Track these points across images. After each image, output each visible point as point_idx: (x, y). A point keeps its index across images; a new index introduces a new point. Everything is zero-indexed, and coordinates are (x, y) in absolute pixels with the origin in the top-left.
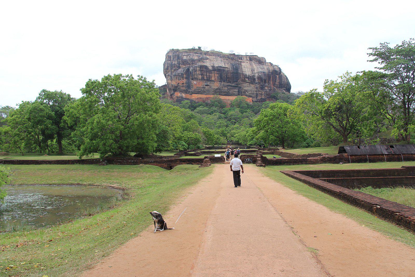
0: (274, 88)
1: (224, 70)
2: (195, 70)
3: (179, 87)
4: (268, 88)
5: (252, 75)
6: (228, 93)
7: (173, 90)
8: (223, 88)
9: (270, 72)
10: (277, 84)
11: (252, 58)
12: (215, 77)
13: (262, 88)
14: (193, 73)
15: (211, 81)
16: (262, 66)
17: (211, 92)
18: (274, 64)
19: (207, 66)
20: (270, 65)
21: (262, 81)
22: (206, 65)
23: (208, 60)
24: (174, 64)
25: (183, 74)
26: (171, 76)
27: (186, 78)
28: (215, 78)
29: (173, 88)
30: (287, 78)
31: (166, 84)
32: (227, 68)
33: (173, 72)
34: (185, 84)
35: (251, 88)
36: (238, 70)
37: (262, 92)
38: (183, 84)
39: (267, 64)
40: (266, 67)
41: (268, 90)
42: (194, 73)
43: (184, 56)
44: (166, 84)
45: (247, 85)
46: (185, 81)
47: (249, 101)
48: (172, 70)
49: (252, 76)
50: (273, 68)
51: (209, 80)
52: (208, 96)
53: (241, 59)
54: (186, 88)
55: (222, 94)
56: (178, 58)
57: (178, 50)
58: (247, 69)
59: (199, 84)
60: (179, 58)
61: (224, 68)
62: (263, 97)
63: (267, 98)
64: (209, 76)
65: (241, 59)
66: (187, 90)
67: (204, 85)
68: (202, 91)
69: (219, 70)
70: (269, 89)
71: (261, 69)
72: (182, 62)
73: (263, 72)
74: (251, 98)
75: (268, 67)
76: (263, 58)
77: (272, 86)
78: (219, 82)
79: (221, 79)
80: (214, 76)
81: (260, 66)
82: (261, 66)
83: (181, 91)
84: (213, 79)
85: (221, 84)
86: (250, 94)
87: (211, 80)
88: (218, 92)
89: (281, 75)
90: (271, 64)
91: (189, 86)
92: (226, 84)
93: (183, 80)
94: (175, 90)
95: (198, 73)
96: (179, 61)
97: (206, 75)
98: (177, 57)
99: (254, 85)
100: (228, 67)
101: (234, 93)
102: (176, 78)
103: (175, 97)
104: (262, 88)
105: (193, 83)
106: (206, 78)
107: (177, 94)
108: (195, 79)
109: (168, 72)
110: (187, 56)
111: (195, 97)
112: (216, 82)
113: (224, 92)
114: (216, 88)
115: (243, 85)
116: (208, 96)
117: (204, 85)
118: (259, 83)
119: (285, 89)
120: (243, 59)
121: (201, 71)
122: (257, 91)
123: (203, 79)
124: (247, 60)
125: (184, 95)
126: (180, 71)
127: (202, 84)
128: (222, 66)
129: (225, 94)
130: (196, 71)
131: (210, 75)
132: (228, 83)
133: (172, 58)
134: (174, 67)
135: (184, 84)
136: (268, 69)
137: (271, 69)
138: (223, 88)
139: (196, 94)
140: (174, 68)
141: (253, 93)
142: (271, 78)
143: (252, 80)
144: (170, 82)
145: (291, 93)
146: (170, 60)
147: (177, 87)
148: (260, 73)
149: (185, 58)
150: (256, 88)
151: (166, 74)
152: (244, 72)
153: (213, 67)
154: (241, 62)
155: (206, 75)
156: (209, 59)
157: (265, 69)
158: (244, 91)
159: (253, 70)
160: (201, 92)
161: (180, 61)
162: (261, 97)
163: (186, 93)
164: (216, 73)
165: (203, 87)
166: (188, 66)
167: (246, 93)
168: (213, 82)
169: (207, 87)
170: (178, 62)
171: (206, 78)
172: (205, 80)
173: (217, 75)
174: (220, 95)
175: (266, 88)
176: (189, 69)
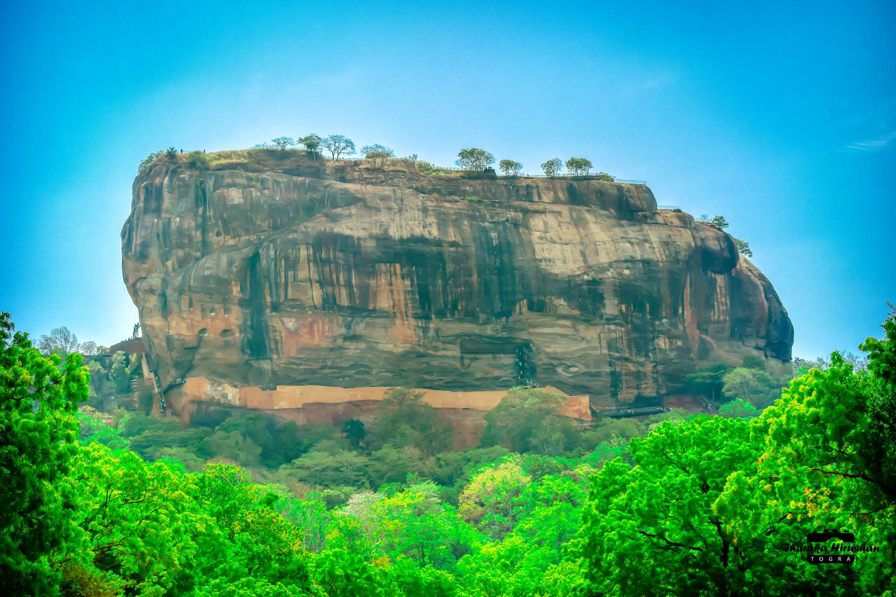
0: (702, 341)
1: (440, 256)
2: (287, 258)
3: (203, 350)
4: (671, 343)
5: (586, 277)
6: (462, 375)
7: (177, 365)
8: (436, 349)
9: (678, 261)
10: (718, 322)
11: (583, 193)
12: (392, 292)
14: (278, 274)
15: (374, 313)
16: (636, 228)
17: (374, 372)
18: (697, 218)
19: (349, 237)
20: (676, 222)
21: (640, 308)
22: (347, 232)
23: (353, 210)
24: (180, 232)
25: (223, 283)
26: (163, 296)
27: (242, 303)
28: (395, 297)
29: (174, 355)
30: (769, 289)
31: (140, 334)
32: (453, 244)
33: (174, 270)
34: (237, 335)
35: (584, 345)
36: (511, 253)
37: (642, 365)
38: (226, 332)
39: (660, 219)
40: (654, 235)
41: (673, 355)
42: (286, 278)
43: (229, 186)
44: (140, 334)
46: (235, 317)
47: (576, 416)
48: (169, 263)
49: (588, 281)
50: (694, 237)
53: (529, 197)
54: (243, 351)
55: (431, 381)
56: (197, 199)
57: (196, 162)
58: (560, 245)
59: (311, 332)
60: (201, 199)
61: (438, 243)
62: (649, 391)
63: (667, 394)
65: (529, 197)
66: (246, 363)
68: (331, 367)
69: (412, 256)
70: (678, 348)
71: (632, 244)
72: (222, 218)
74: (585, 400)
75: (665, 232)
76: (641, 186)
77: (695, 334)
78: (416, 317)
79: (425, 304)
81: (626, 233)
82: (632, 232)
83: (219, 374)
84: (384, 303)
85: (425, 330)
86: (576, 375)
87: (374, 310)
88: (413, 369)
89: (740, 273)
90: (685, 220)
91: (258, 344)
92: (453, 327)
93: (227, 311)
94: (186, 368)
96: (204, 212)
97: (349, 285)
98: (192, 193)
99: (599, 329)
100: (458, 239)
101: (497, 373)
102: (191, 304)
103: (184, 400)
104: (641, 341)
105: (279, 326)
106: (344, 301)
108: (291, 307)
109: (149, 271)
110: (244, 187)
111: (288, 399)
112: (398, 322)
113: (444, 371)
114: (400, 349)
118: (623, 319)
120: (536, 199)
121: (318, 261)
122: (618, 359)
123: (330, 304)
124: (556, 201)
125: (232, 393)
126: (210, 266)
127: (324, 332)
128: (427, 236)
129: (449, 379)
130: (292, 264)
131: (367, 287)
132: (461, 320)
133: (167, 203)
134: (181, 246)
136: (666, 244)
137: (684, 239)
138: (436, 349)
140: (180, 253)
141: (593, 370)
142: (687, 291)
143: (585, 296)
144: (157, 321)
147: (193, 349)
148: (628, 268)
149: (235, 196)
150: (611, 345)
151: (134, 285)
152: (543, 265)
153: (383, 240)
154: (525, 211)
155: (349, 285)
156: (363, 200)
157: (655, 245)
158: (546, 360)
159: (586, 250)
160: (326, 371)
161: (210, 213)
162: (636, 392)
164: (398, 271)
165: (332, 350)
166: (253, 238)
167: (559, 370)
168: (386, 321)
169: (353, 349)
170: (200, 220)
171: (344, 301)
172: (341, 308)
173: (403, 285)
174: (422, 384)
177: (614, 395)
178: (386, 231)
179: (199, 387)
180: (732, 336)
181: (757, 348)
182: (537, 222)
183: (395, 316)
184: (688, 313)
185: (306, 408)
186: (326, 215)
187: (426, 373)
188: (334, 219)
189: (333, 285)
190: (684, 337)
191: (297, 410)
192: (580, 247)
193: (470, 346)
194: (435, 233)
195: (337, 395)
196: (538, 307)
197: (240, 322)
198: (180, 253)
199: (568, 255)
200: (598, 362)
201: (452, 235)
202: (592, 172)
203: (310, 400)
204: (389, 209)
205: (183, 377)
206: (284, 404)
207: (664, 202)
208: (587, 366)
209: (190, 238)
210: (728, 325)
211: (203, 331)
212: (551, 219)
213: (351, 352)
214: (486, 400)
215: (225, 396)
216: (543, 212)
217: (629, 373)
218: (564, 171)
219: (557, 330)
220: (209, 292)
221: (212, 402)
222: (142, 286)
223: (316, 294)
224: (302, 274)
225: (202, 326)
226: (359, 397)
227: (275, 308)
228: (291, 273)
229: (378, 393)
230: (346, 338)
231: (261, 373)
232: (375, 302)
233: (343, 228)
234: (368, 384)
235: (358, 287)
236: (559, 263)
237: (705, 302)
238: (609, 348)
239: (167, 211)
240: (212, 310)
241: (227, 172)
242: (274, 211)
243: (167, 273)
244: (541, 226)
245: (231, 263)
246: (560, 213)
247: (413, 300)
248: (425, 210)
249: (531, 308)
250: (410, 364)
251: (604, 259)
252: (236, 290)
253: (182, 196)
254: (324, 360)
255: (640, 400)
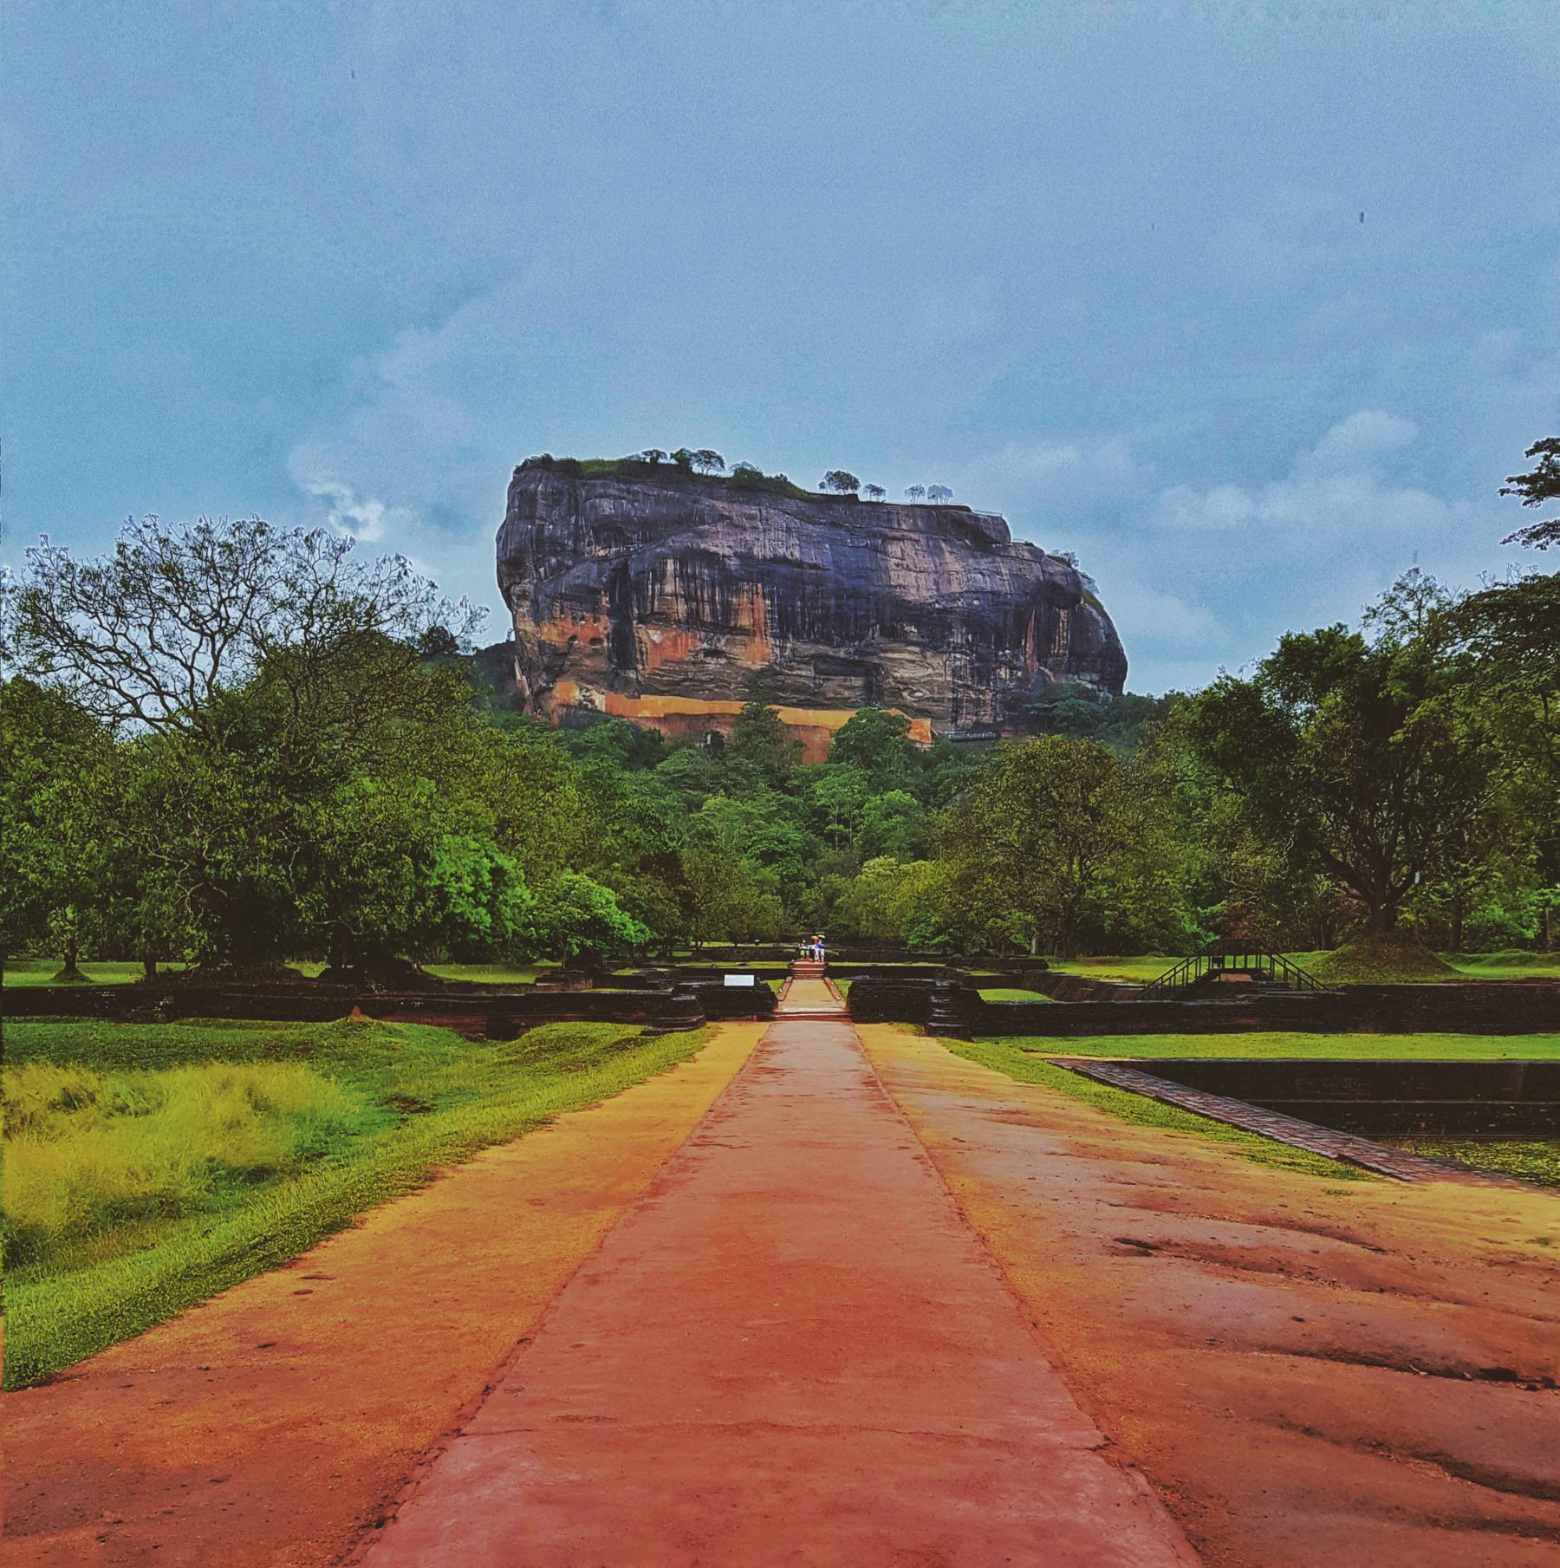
6: (815, 694)
7: (547, 669)
13: (983, 673)
20: (1027, 555)
22: (713, 549)
27: (610, 614)
29: (546, 659)
35: (930, 671)
37: (983, 692)
38: (594, 641)
41: (1012, 685)
43: (601, 496)
45: (907, 656)
46: (604, 626)
51: (724, 625)
52: (717, 707)
58: (914, 573)
61: (800, 564)
62: (987, 719)
64: (727, 605)
67: (697, 653)
70: (1019, 679)
73: (993, 593)
74: (927, 722)
75: (1016, 566)
78: (774, 636)
79: (785, 625)
80: (753, 607)
82: (984, 564)
85: (783, 649)
86: (920, 700)
88: (766, 687)
90: (1037, 554)
91: (623, 649)
92: (807, 649)
94: (555, 673)
95: (669, 588)
101: (846, 694)
103: (553, 704)
104: (983, 673)
105: (645, 638)
107: (567, 691)
109: (523, 577)
110: (615, 498)
111: (651, 708)
112: (757, 639)
114: (757, 667)
115: (890, 655)
116: (717, 707)
117: (697, 653)
119: (1096, 677)
123: (693, 621)
125: (600, 700)
132: (816, 642)
133: (541, 511)
134: (555, 554)
135: (600, 641)
137: (1035, 573)
138: (792, 668)
139: (662, 693)
140: (553, 560)
143: (932, 626)
144: (529, 626)
145: (1125, 692)
146: (531, 518)
147: (564, 655)
150: (955, 673)
151: (508, 589)
153: (746, 558)
155: (712, 601)
163: (611, 687)
165: (694, 663)
167: (905, 694)
168: (746, 639)
169: (713, 664)
172: (704, 624)
173: (764, 604)
174: (776, 701)
175: (1003, 673)
176: (625, 567)
177: (954, 720)
178: (751, 549)
179: (569, 692)
180: (1068, 671)
181: (1091, 682)
182: (894, 549)
183: (755, 634)
184: (1030, 648)
185: (666, 719)
186: (695, 532)
187: (783, 691)
188: (701, 535)
189: (696, 599)
190: (1024, 669)
191: (659, 719)
192: (933, 576)
193: (823, 667)
194: (797, 554)
195: (696, 706)
196: (894, 635)
197: (610, 630)
198: (553, 560)
199: (922, 582)
200: (941, 688)
201: (812, 557)
202: (951, 502)
203: (672, 710)
204: (755, 528)
205: (554, 682)
206: (647, 713)
207: (1015, 537)
208: (932, 692)
209: (562, 545)
210: (1066, 659)
211: (574, 638)
212: (909, 548)
213: (711, 667)
214: (837, 719)
215: (592, 702)
216: (902, 539)
217: (970, 701)
218: (923, 500)
219: (907, 656)
220: (579, 600)
221: (581, 706)
222: (517, 589)
223: (681, 608)
224: (669, 588)
225: (572, 632)
226: (717, 710)
227: (641, 620)
228: (658, 586)
229: (735, 707)
230: (708, 653)
231: (628, 681)
232: (736, 620)
233: (709, 545)
234: (727, 698)
235: (722, 604)
236: (913, 591)
237: (1046, 637)
238: (954, 676)
239: (541, 518)
240: (582, 618)
241: (599, 482)
242: (645, 524)
243: (540, 579)
244: (899, 554)
245: (601, 574)
246: (917, 541)
247: (772, 619)
248: (789, 530)
249: (882, 634)
250: (768, 681)
251: (955, 588)
252: (605, 600)
253: (557, 503)
254: (686, 672)
255: (978, 727)
